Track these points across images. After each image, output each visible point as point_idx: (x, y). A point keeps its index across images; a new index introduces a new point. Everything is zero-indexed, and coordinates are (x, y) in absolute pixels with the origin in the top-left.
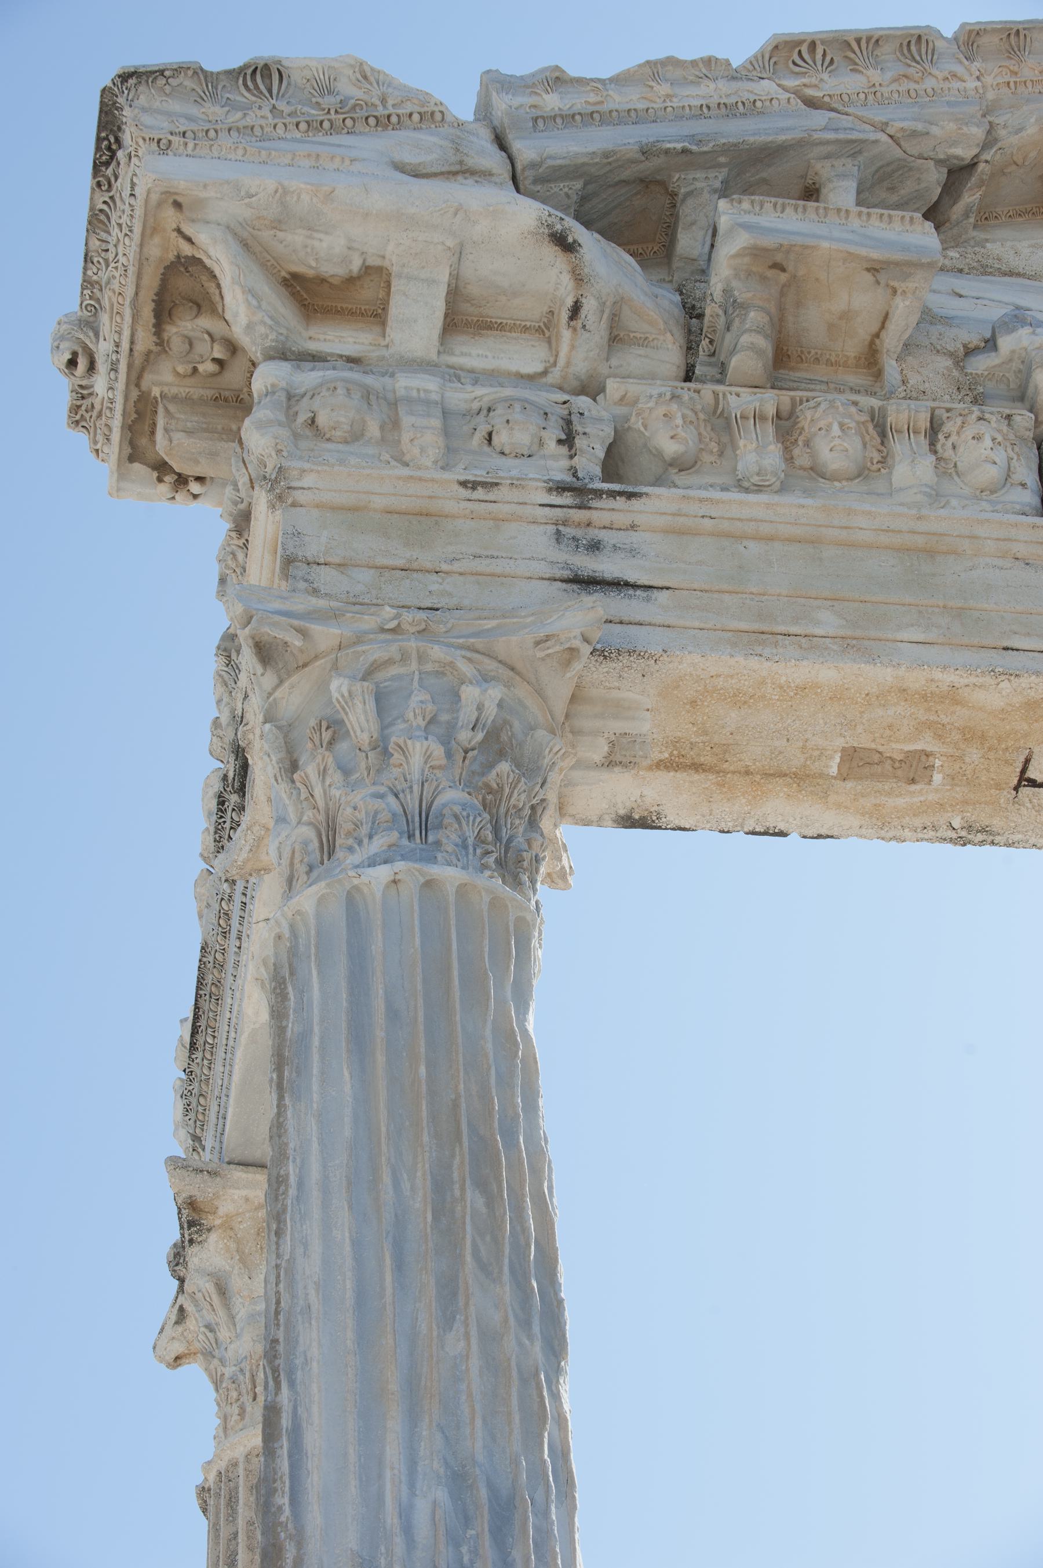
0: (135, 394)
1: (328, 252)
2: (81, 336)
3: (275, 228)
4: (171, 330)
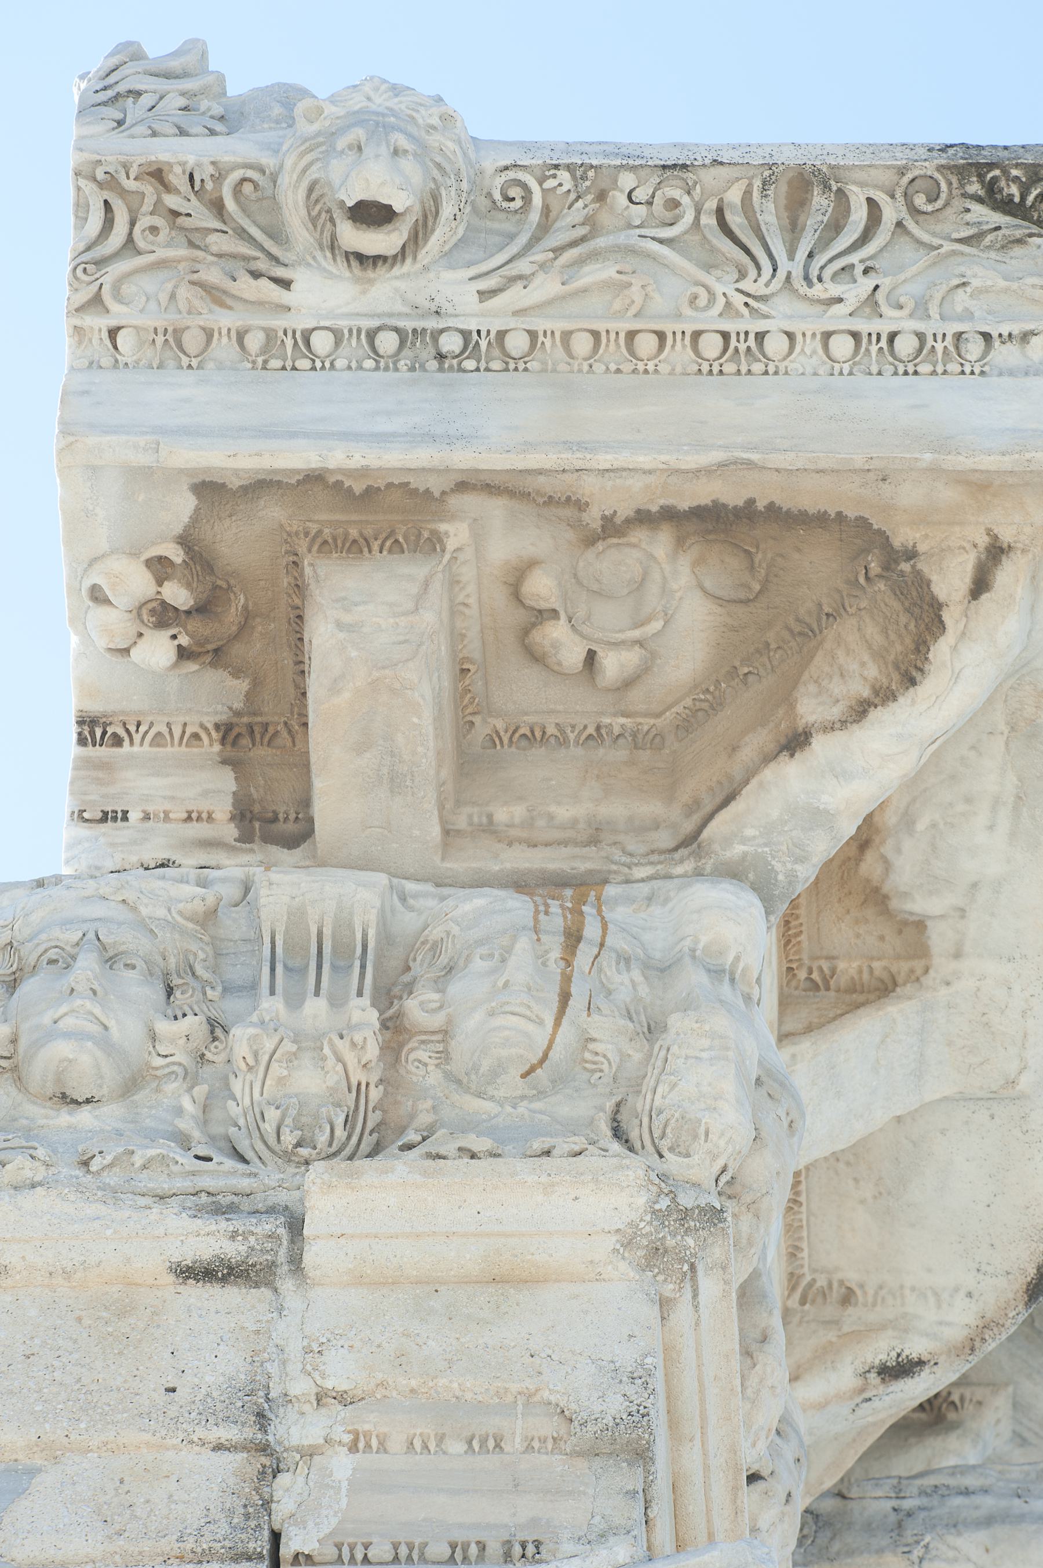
0: (436, 485)
2: (447, 210)
3: (1013, 729)
4: (660, 544)
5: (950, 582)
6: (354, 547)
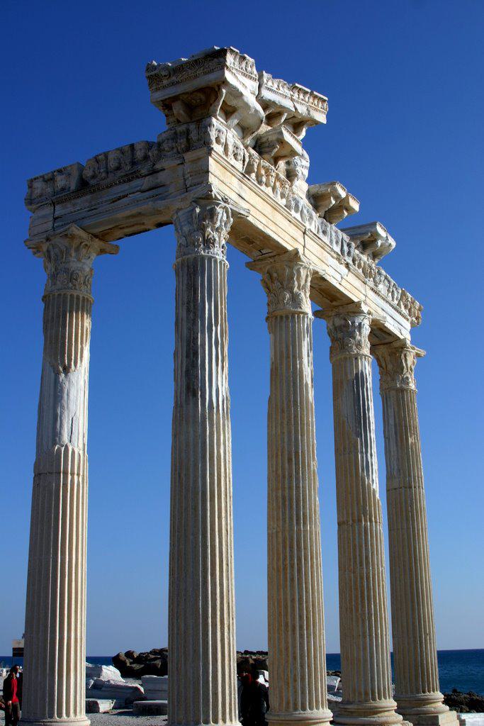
1: (233, 103)
5: (217, 90)
6: (174, 101)
